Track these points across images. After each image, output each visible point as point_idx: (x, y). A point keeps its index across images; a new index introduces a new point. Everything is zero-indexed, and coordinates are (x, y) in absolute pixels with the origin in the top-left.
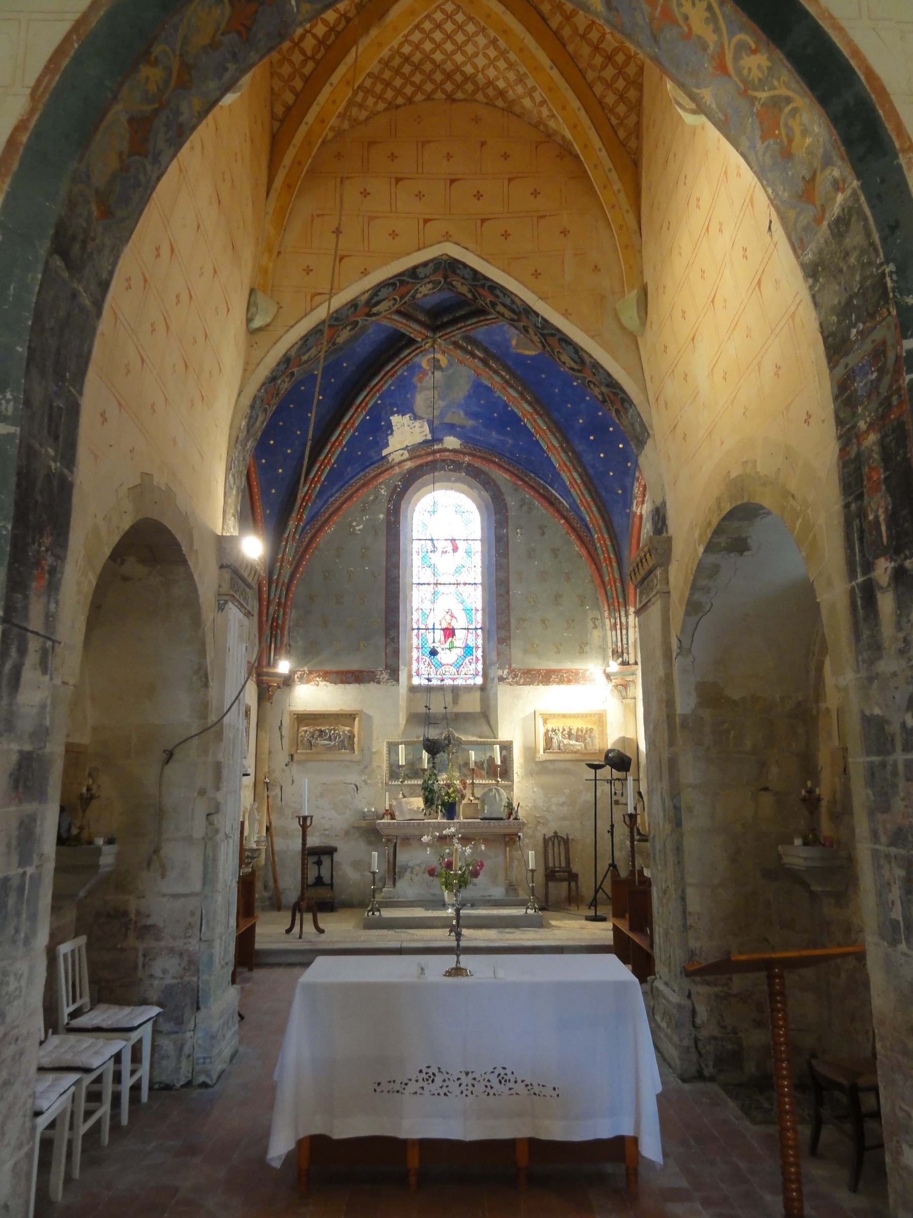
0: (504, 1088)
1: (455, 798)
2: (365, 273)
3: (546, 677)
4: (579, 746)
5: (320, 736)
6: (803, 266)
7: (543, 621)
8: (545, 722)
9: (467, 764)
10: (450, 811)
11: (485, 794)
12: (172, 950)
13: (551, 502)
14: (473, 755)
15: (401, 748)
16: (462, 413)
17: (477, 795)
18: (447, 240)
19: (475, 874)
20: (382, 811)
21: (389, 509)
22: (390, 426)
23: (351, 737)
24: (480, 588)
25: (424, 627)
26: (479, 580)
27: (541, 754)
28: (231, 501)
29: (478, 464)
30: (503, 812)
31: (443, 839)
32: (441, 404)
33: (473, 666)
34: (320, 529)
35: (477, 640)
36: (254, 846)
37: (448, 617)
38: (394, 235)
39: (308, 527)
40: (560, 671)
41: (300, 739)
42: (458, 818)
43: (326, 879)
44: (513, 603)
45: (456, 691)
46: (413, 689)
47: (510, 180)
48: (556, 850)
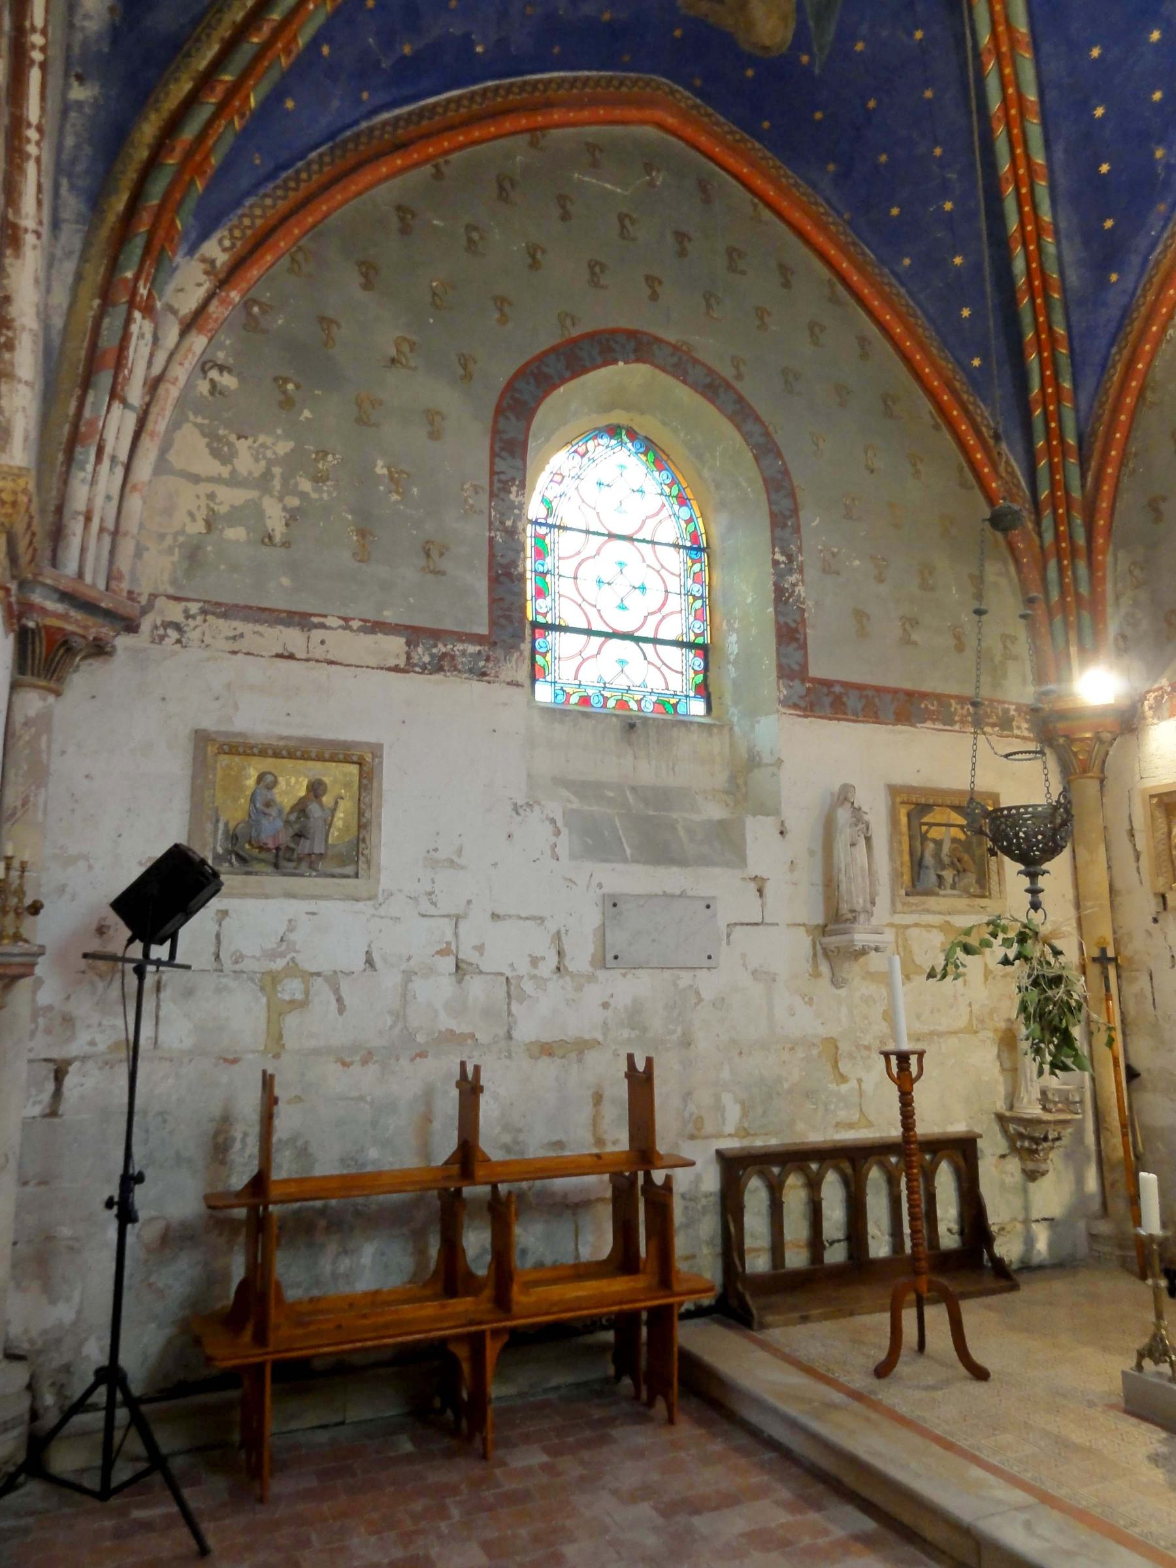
36: (1036, 1111)
39: (1114, 350)
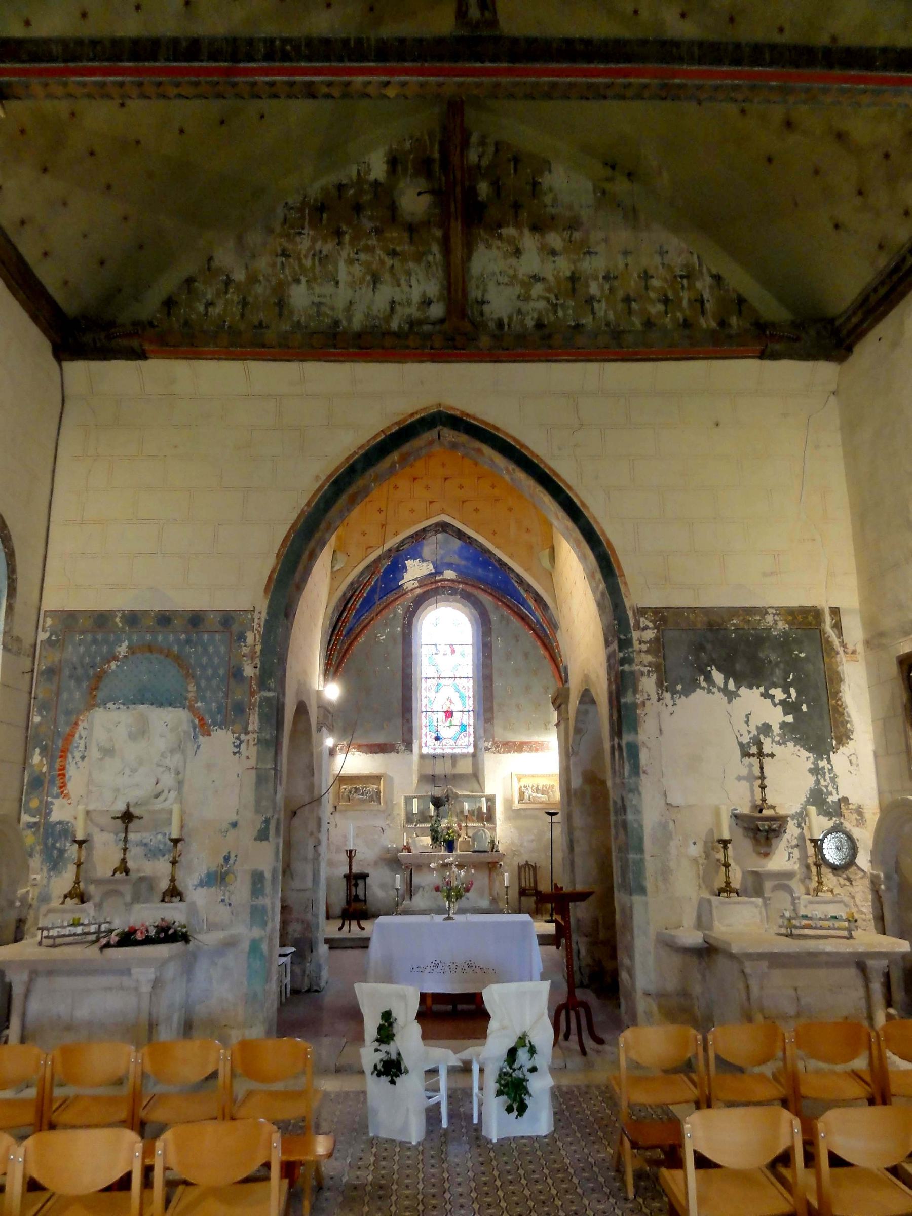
0: (470, 970)
1: (453, 837)
2: (396, 534)
3: (519, 747)
4: (544, 798)
5: (355, 792)
6: (596, 601)
7: (518, 706)
8: (519, 780)
9: (462, 812)
10: (450, 846)
11: (475, 834)
12: (298, 920)
13: (523, 618)
14: (466, 806)
15: (415, 800)
16: (456, 557)
17: (470, 835)
18: (443, 513)
19: (467, 890)
20: (401, 847)
21: (404, 624)
22: (405, 568)
23: (378, 793)
24: (471, 681)
25: (430, 710)
26: (471, 675)
27: (516, 805)
28: (321, 667)
29: (469, 589)
30: (487, 846)
31: (446, 866)
32: (442, 552)
33: (467, 739)
34: (355, 638)
35: (469, 719)
37: (448, 703)
38: (412, 511)
40: (530, 742)
41: (341, 794)
42: (456, 851)
43: (362, 897)
44: (495, 693)
45: (454, 758)
46: (423, 757)
47: (479, 478)
48: (527, 874)
